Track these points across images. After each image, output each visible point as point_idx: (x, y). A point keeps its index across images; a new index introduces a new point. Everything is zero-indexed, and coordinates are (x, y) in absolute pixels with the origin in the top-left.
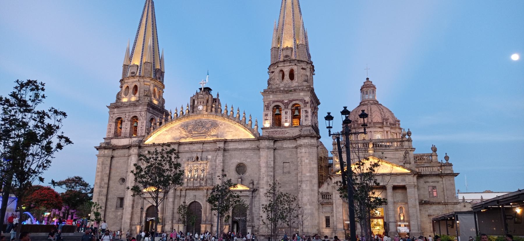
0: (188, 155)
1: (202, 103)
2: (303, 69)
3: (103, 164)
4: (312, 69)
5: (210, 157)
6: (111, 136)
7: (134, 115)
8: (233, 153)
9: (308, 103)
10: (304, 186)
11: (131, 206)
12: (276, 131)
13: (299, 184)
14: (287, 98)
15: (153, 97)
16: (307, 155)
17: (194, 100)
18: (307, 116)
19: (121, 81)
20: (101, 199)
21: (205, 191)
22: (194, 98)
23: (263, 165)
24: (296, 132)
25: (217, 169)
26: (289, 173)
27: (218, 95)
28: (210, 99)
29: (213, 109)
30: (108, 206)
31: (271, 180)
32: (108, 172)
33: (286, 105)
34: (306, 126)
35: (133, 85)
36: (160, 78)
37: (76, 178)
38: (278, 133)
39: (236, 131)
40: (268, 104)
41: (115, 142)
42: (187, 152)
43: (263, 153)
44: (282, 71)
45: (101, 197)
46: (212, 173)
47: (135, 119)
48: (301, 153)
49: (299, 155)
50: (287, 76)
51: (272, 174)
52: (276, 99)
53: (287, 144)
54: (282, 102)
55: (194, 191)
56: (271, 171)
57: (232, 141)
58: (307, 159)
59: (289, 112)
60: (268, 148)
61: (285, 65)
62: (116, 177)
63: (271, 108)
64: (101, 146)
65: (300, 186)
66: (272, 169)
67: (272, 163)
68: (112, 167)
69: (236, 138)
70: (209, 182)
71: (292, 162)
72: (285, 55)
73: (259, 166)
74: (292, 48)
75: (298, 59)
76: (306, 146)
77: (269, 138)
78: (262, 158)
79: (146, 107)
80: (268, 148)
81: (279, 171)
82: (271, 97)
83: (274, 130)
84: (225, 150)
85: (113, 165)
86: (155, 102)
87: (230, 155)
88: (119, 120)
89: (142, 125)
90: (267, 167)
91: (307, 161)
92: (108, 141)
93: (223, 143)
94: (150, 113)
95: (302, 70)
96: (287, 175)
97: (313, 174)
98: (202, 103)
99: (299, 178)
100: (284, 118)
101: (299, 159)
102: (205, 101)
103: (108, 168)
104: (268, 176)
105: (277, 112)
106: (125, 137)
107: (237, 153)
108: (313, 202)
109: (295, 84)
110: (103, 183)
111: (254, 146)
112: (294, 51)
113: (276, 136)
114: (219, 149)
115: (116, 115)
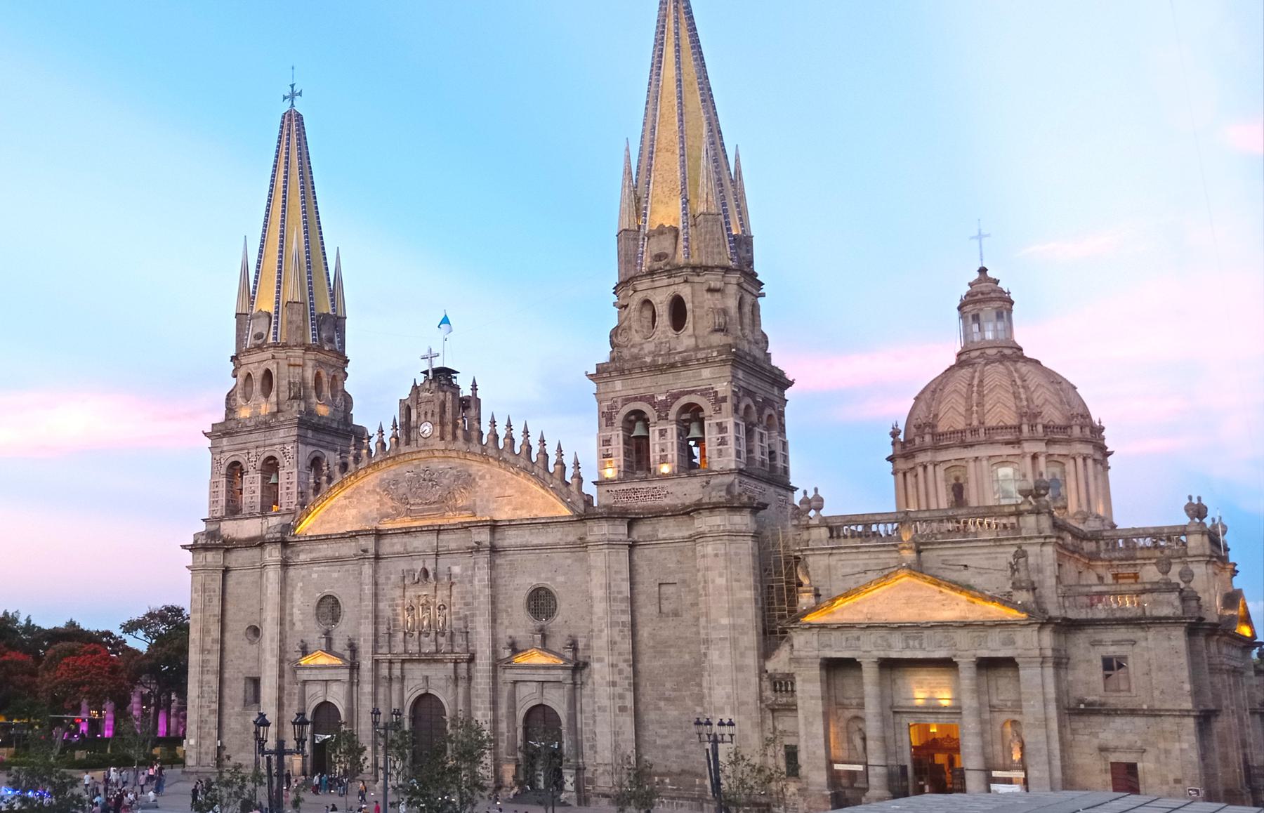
0: (403, 565)
2: (710, 290)
3: (204, 591)
4: (751, 282)
5: (456, 570)
6: (218, 515)
7: (267, 454)
9: (724, 399)
10: (714, 655)
11: (275, 702)
12: (636, 491)
13: (703, 648)
14: (664, 389)
15: (314, 400)
16: (721, 562)
17: (409, 409)
18: (723, 442)
19: (234, 359)
20: (208, 682)
21: (451, 665)
22: (408, 402)
23: (599, 593)
24: (690, 491)
25: (476, 604)
26: (676, 614)
27: (474, 387)
28: (449, 405)
29: (459, 433)
30: (227, 700)
31: (624, 637)
32: (218, 610)
33: (663, 408)
34: (721, 473)
35: (260, 372)
36: (331, 340)
37: (168, 609)
38: (641, 495)
39: (522, 493)
40: (611, 407)
41: (231, 529)
42: (397, 555)
43: (598, 559)
44: (647, 302)
45: (206, 677)
47: (271, 466)
48: (703, 556)
49: (701, 563)
50: (664, 319)
51: (626, 618)
52: (632, 392)
53: (669, 530)
54: (650, 399)
55: (422, 666)
56: (623, 612)
57: (511, 524)
58: (721, 575)
59: (672, 430)
60: (611, 543)
61: (657, 284)
62: (237, 626)
63: (619, 419)
64: (196, 541)
65: (705, 655)
66: (625, 606)
67: (626, 587)
68: (228, 597)
69: (524, 514)
70: (459, 639)
71: (684, 581)
72: (656, 251)
73: (589, 598)
74: (676, 230)
75: (694, 260)
76: (716, 536)
77: (611, 515)
78: (593, 572)
79: (295, 431)
80: (611, 543)
81: (647, 610)
82: (618, 385)
83: (629, 486)
84: (494, 550)
85: (229, 589)
86: (323, 410)
87: (511, 564)
88: (235, 470)
89: (289, 479)
90: (610, 599)
91: (721, 581)
92: (213, 527)
93: (487, 530)
94: (307, 444)
95: (708, 296)
96: (671, 622)
97: (741, 621)
99: (702, 631)
100: (657, 448)
101: (700, 574)
102: (437, 410)
103: (216, 602)
104: (613, 624)
105: (639, 431)
106: (252, 516)
108: (742, 703)
109: (685, 340)
110: (209, 639)
111: (571, 538)
112: (681, 237)
113: (638, 503)
114: (477, 548)
115: (228, 455)
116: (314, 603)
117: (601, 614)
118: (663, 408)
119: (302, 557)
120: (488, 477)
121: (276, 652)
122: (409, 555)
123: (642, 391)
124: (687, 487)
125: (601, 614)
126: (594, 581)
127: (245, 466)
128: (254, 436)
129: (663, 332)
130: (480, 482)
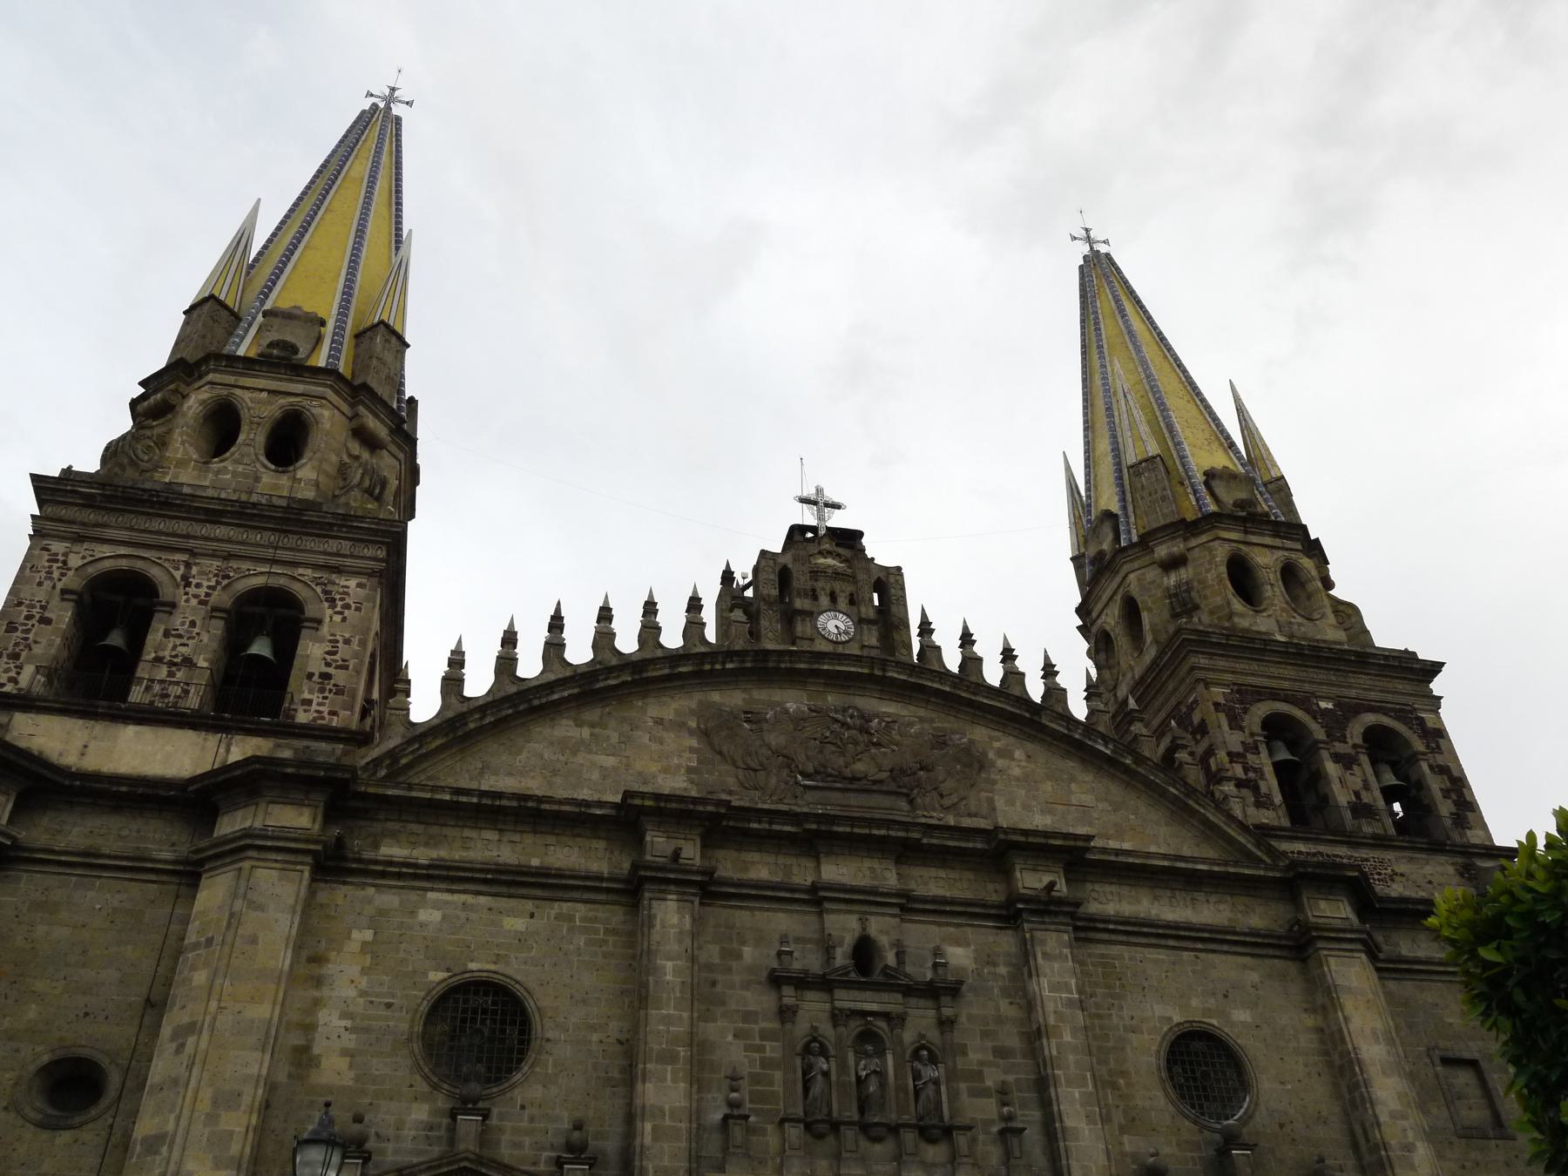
0: (782, 922)
1: (842, 602)
5: (959, 956)
8: (1125, 952)
22: (787, 560)
25: (1051, 1048)
33: (1336, 723)
41: (56, 739)
46: (1003, 1093)
52: (1265, 682)
78: (1348, 1003)
98: (842, 602)
107: (1153, 961)
114: (1047, 907)
115: (106, 550)
116: (417, 1000)
117: (1394, 1105)
118: (1336, 723)
119: (392, 850)
120: (1018, 754)
121: (239, 1147)
122: (817, 898)
123: (1286, 685)
124: (1428, 869)
125: (1394, 1105)
126: (1356, 1023)
127: (167, 592)
128: (220, 531)
129: (1283, 610)
130: (1000, 763)
